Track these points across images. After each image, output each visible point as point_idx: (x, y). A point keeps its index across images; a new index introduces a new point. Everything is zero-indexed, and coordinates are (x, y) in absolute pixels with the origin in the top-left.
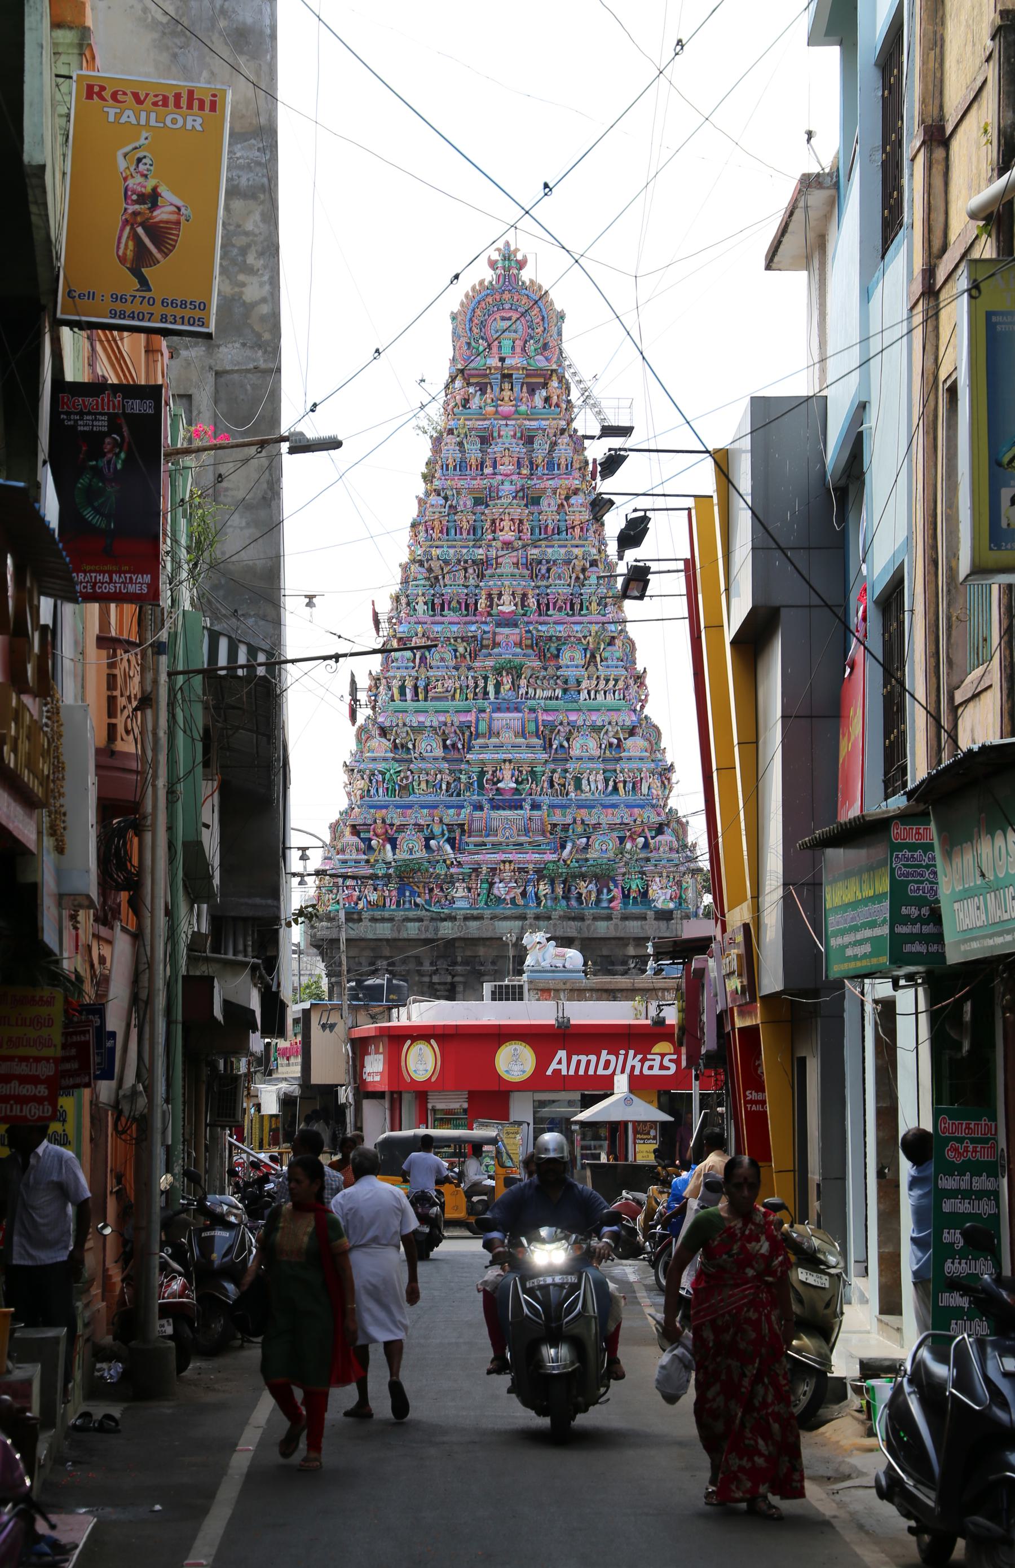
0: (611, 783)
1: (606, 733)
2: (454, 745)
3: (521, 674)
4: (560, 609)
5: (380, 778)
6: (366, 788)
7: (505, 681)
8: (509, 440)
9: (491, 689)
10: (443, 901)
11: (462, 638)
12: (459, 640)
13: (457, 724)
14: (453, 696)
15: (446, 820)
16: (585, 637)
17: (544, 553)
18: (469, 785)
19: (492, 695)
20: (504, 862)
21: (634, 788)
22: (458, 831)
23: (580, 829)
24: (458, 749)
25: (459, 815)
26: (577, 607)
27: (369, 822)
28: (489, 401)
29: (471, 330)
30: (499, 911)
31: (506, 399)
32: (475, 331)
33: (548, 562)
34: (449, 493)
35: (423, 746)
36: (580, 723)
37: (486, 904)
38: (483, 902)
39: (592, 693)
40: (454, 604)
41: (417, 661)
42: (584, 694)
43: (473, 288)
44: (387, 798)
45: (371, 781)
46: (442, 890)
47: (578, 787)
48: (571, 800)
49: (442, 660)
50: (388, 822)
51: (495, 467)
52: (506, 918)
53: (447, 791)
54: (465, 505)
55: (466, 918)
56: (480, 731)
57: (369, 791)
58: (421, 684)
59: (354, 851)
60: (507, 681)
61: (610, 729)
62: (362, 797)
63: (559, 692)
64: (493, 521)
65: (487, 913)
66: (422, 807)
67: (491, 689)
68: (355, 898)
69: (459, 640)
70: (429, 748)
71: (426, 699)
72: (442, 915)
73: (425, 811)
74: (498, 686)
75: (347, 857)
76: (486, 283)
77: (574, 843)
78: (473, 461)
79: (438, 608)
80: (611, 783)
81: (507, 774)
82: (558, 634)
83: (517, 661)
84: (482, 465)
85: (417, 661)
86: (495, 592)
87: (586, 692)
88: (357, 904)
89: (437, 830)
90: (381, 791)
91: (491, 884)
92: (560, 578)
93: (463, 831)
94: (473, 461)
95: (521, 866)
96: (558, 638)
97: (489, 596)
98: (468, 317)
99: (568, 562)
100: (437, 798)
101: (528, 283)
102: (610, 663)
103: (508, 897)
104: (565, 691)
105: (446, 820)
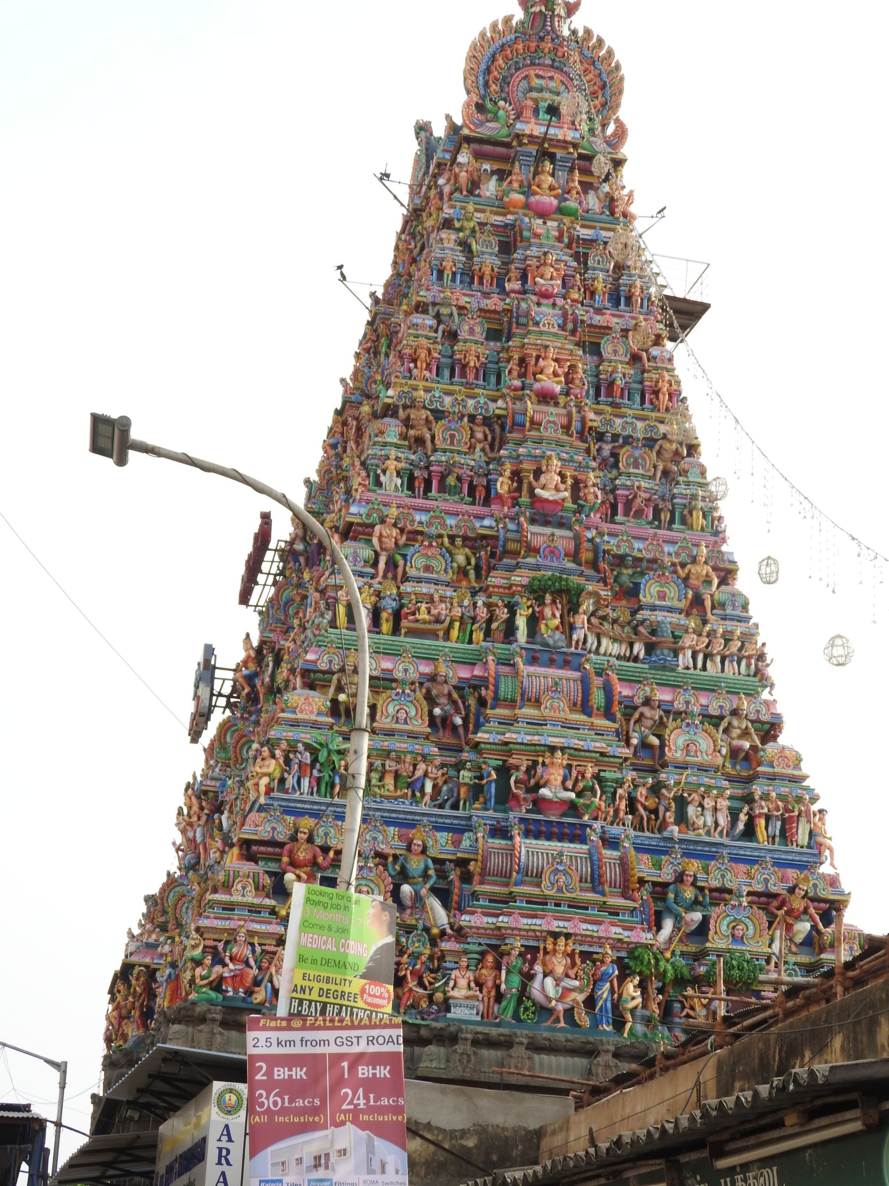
0: (743, 818)
1: (726, 731)
2: (445, 720)
3: (578, 605)
4: (639, 514)
5: (307, 758)
6: (277, 774)
7: (548, 611)
8: (552, 242)
9: (521, 622)
10: (424, 1004)
11: (465, 538)
12: (459, 541)
13: (454, 682)
14: (447, 637)
15: (433, 852)
16: (683, 565)
17: (609, 423)
18: (477, 791)
19: (522, 634)
20: (555, 935)
21: (783, 832)
22: (454, 876)
23: (689, 894)
24: (455, 728)
25: (457, 843)
26: (665, 516)
27: (281, 838)
28: (516, 185)
29: (486, 85)
30: (544, 1033)
31: (546, 186)
32: (493, 87)
33: (615, 437)
34: (444, 311)
35: (391, 709)
36: (679, 706)
37: (516, 1016)
38: (510, 1014)
39: (700, 657)
40: (451, 480)
41: (382, 565)
42: (685, 659)
43: (494, 26)
44: (316, 798)
45: (288, 761)
46: (421, 984)
47: (682, 819)
48: (671, 839)
49: (428, 568)
50: (319, 841)
51: (524, 278)
52: (552, 1049)
53: (433, 798)
54: (472, 331)
55: (478, 1042)
56: (502, 694)
57: (282, 780)
58: (389, 605)
59: (250, 888)
60: (552, 617)
61: (735, 723)
62: (269, 790)
63: (639, 648)
64: (522, 361)
65: (522, 1034)
66: (388, 823)
67: (521, 622)
68: (249, 981)
69: (459, 541)
70: (402, 715)
71: (396, 630)
72: (424, 1032)
73: (391, 830)
74: (533, 621)
75: (236, 898)
76: (514, 23)
77: (678, 919)
78: (487, 271)
79: (420, 486)
80: (743, 818)
81: (556, 775)
82: (636, 553)
83: (575, 580)
84: (500, 280)
85: (382, 565)
86: (528, 466)
87: (689, 653)
88: (250, 993)
89: (416, 865)
90: (305, 782)
91: (529, 977)
92: (636, 465)
93: (467, 878)
94: (487, 271)
95: (586, 948)
96: (638, 560)
97: (516, 475)
98: (483, 66)
99: (650, 442)
100: (414, 808)
101: (581, 33)
102: (729, 611)
103: (560, 1007)
104: (650, 648)
105: (433, 852)
